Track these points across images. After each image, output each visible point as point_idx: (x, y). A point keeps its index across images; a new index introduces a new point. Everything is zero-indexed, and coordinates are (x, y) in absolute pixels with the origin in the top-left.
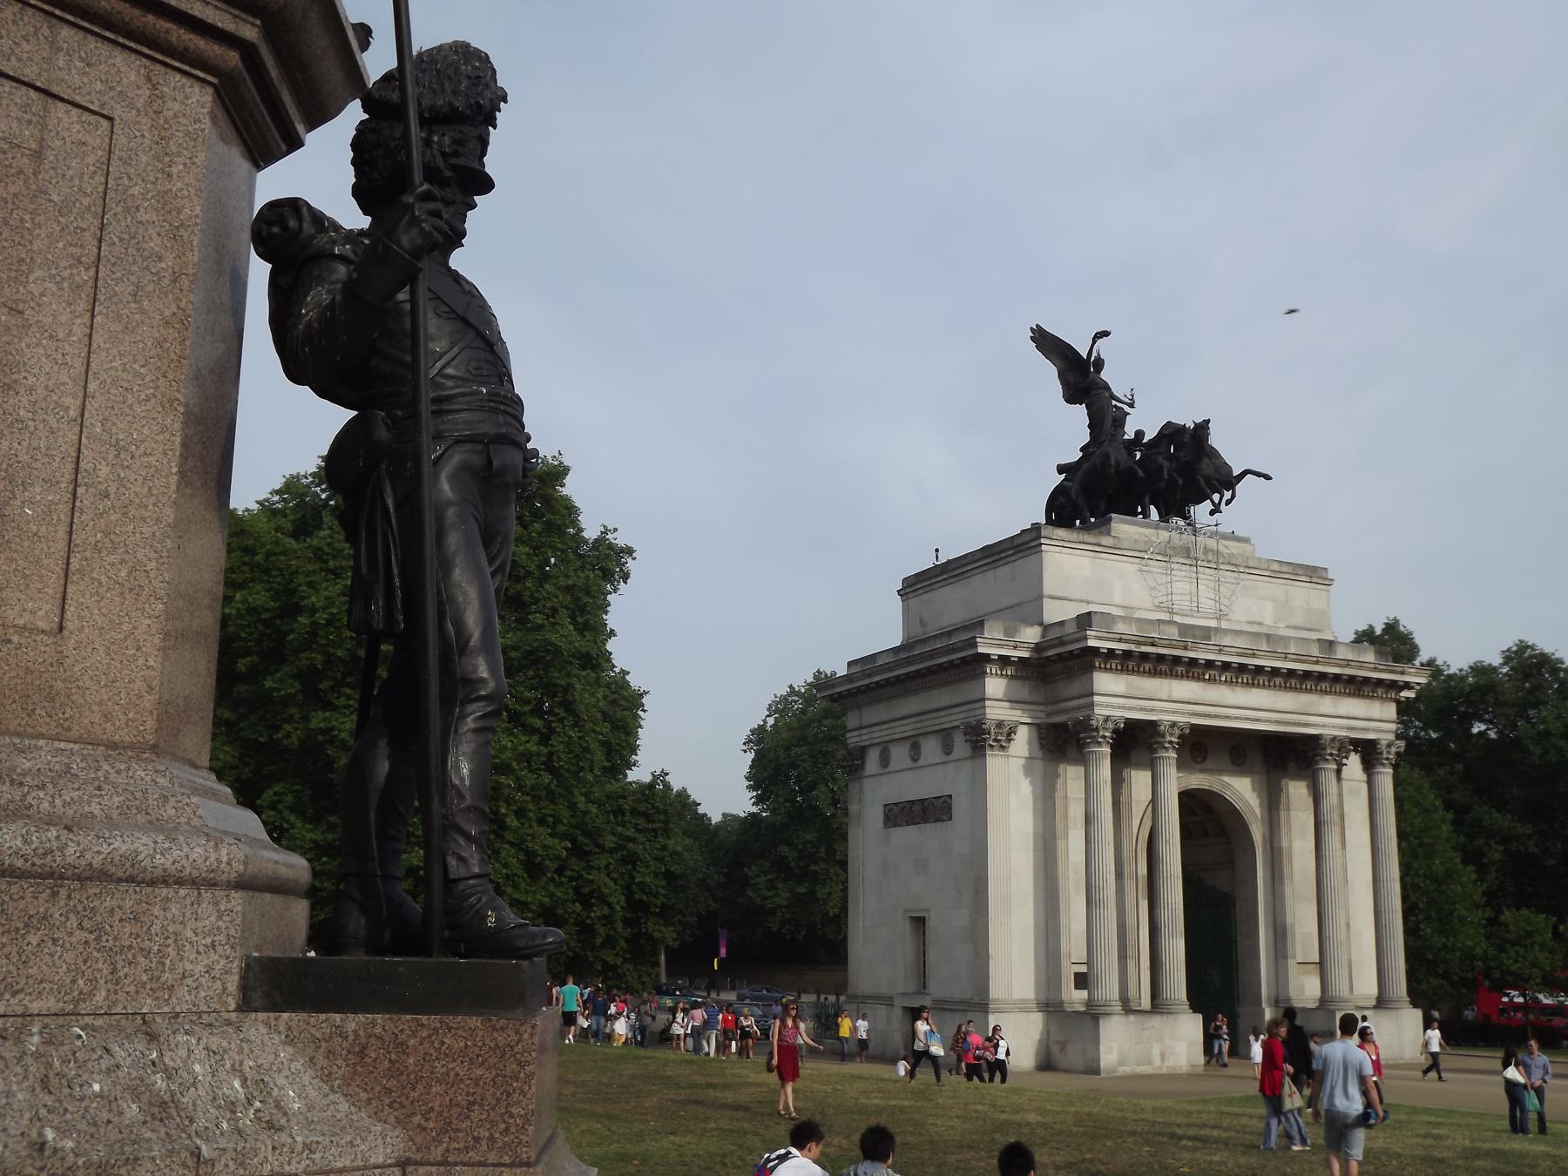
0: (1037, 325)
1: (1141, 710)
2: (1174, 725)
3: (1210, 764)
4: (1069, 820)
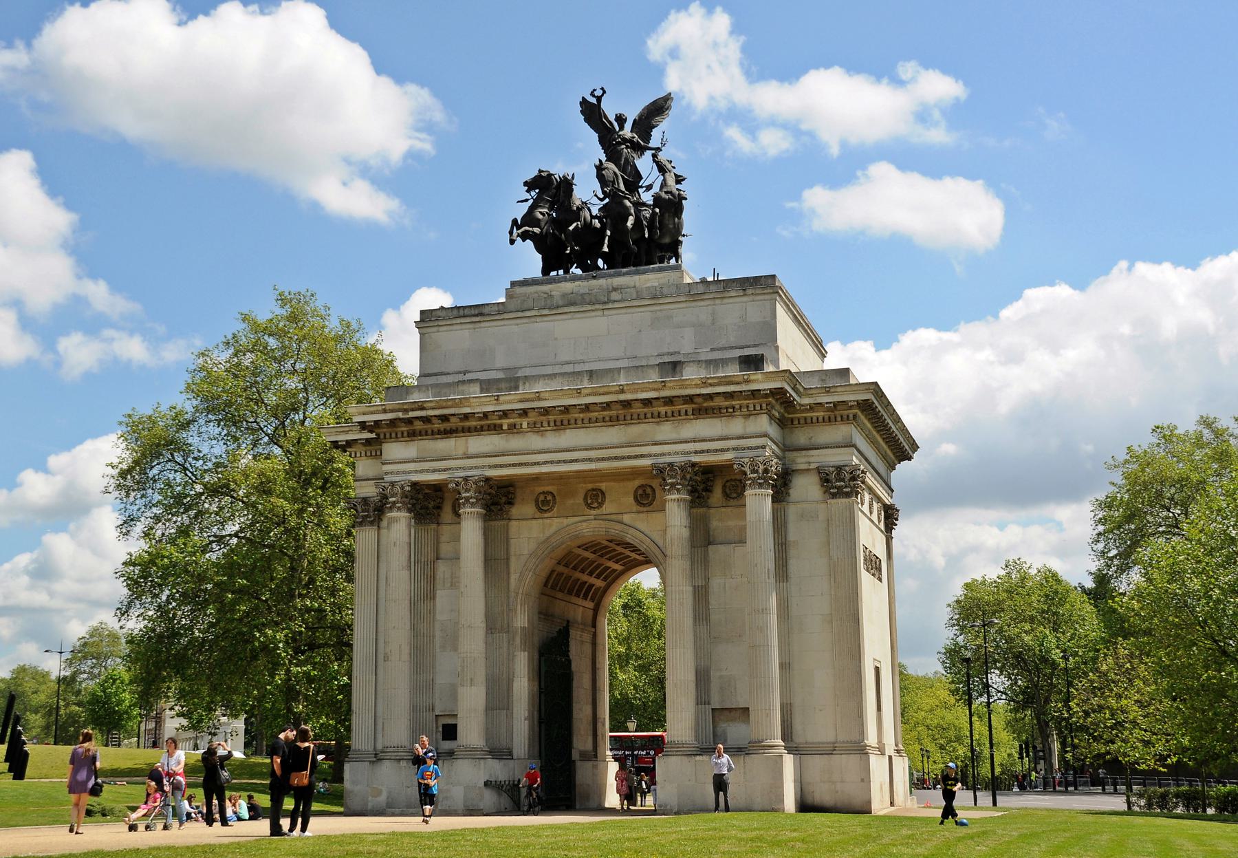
0: (583, 98)
1: (434, 471)
2: (466, 479)
3: (608, 508)
4: (437, 581)
